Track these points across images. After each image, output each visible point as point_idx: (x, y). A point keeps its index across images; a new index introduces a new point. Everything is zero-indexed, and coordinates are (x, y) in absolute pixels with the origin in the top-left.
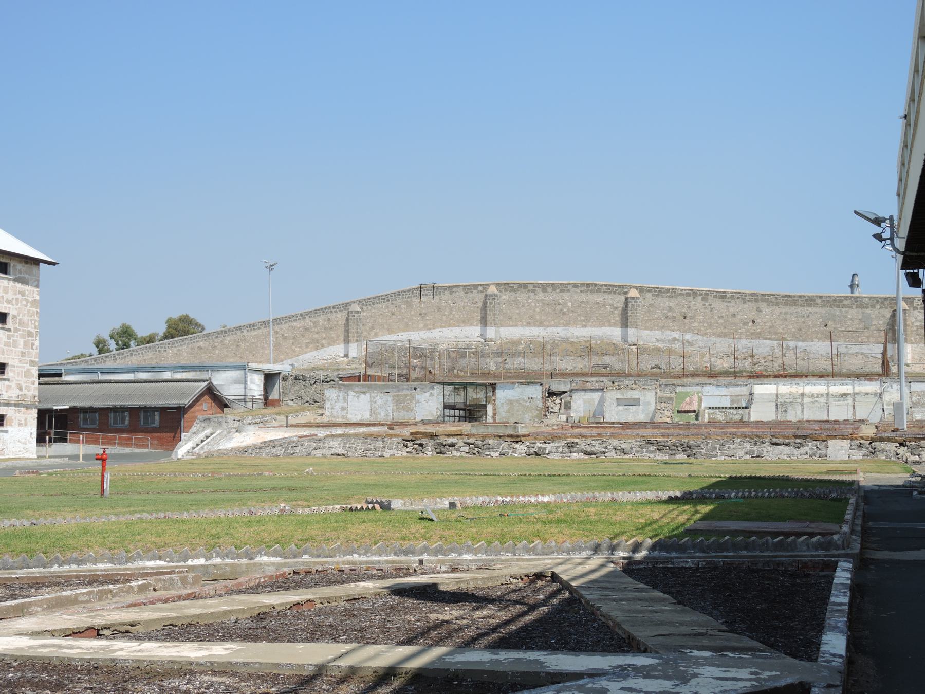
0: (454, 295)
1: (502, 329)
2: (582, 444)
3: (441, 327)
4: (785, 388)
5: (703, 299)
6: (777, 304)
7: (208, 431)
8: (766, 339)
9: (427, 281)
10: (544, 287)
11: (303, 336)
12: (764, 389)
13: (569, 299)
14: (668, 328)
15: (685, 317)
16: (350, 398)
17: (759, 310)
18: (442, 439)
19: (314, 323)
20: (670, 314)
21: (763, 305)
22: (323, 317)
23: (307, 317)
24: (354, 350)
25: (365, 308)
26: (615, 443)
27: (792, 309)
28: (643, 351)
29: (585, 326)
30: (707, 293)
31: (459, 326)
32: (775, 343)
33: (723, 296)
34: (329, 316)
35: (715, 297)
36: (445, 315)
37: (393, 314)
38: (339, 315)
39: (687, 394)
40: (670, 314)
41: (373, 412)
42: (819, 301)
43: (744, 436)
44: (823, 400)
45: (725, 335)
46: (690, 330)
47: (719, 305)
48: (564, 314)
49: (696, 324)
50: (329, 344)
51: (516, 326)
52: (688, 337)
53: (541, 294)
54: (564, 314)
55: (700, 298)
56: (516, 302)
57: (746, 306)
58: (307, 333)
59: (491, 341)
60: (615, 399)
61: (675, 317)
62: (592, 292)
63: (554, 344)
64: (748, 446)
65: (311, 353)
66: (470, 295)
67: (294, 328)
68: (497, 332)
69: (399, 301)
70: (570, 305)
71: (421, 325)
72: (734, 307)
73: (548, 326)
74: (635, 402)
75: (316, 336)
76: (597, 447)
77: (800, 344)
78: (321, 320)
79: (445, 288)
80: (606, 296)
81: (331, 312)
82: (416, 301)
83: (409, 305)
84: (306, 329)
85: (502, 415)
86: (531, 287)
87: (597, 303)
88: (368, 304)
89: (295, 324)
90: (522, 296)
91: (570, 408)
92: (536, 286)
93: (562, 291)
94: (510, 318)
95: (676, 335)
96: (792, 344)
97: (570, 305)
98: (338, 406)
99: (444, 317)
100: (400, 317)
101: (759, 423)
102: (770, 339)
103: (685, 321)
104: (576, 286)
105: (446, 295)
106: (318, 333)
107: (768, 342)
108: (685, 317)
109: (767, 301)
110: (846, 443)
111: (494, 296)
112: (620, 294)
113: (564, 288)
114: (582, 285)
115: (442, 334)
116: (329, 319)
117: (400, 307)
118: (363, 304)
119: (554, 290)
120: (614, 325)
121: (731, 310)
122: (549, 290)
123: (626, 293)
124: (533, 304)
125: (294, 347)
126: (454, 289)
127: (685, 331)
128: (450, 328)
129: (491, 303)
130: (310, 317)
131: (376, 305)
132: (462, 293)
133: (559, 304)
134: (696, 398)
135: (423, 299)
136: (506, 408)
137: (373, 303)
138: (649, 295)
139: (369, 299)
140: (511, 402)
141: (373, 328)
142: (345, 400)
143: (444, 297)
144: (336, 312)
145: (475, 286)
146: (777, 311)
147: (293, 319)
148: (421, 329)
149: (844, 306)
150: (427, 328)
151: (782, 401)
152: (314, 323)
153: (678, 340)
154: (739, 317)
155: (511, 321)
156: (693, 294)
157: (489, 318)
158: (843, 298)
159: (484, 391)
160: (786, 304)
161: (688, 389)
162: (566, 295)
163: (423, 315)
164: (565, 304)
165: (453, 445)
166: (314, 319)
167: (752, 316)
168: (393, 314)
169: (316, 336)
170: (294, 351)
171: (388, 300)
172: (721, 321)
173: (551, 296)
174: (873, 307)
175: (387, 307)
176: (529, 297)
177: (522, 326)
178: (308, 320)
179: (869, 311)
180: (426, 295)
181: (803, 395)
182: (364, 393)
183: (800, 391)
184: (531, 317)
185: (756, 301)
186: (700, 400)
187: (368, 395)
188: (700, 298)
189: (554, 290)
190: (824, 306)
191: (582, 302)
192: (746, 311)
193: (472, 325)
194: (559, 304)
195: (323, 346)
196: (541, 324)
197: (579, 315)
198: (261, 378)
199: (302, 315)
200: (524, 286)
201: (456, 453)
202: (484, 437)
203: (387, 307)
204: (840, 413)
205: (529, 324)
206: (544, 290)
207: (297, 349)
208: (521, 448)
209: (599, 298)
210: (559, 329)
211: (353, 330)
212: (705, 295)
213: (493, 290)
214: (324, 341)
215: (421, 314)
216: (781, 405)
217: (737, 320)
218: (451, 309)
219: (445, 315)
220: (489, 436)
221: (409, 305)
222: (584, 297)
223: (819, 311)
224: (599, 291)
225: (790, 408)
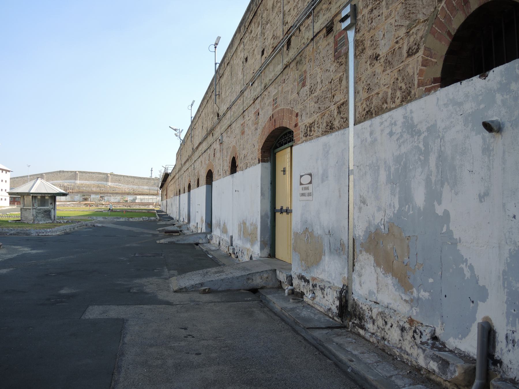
4: (142, 197)
9: (62, 170)
10: (89, 173)
17: (134, 180)
21: (135, 179)
26: (118, 205)
27: (141, 180)
30: (124, 176)
33: (127, 177)
43: (138, 205)
45: (127, 184)
46: (121, 183)
47: (126, 178)
52: (120, 184)
64: (138, 206)
72: (129, 179)
74: (116, 199)
76: (116, 206)
77: (142, 187)
82: (59, 174)
83: (57, 175)
85: (92, 200)
90: (84, 174)
92: (87, 172)
95: (117, 184)
96: (141, 187)
101: (137, 203)
105: (66, 173)
110: (152, 206)
140: (93, 198)
141: (48, 179)
145: (73, 171)
146: (138, 180)
162: (94, 175)
173: (91, 175)
178: (32, 177)
179: (155, 181)
192: (132, 180)
196: (88, 180)
204: (150, 201)
205: (85, 180)
208: (104, 206)
210: (92, 182)
212: (124, 176)
216: (141, 200)
222: (98, 175)
223: (146, 181)
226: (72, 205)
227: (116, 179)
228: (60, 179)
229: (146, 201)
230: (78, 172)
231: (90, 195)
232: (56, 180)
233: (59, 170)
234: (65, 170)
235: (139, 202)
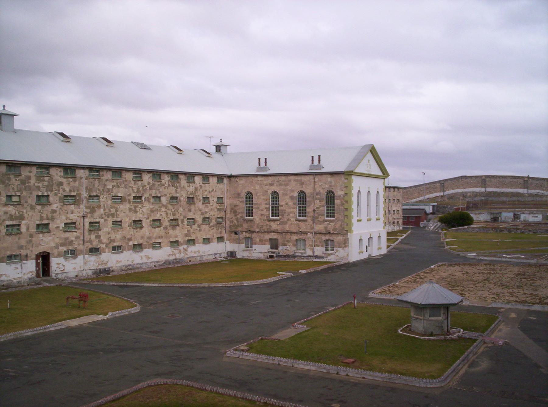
15: (541, 186)
19: (430, 186)
29: (511, 188)
34: (435, 184)
37: (454, 184)
49: (544, 188)
50: (434, 193)
55: (546, 181)
56: (491, 181)
62: (514, 178)
66: (477, 179)
70: (507, 182)
73: (501, 188)
78: (432, 186)
80: (518, 180)
82: (460, 180)
83: (458, 181)
86: (495, 177)
87: (515, 182)
90: (492, 180)
97: (507, 182)
105: (469, 179)
112: (522, 179)
123: (524, 179)
133: (504, 182)
138: (531, 180)
152: (430, 186)
162: (506, 179)
163: (463, 185)
164: (506, 182)
168: (454, 184)
170: (424, 194)
173: (501, 180)
175: (452, 182)
178: (428, 185)
180: (464, 179)
188: (546, 181)
189: (502, 178)
191: (511, 181)
194: (504, 182)
195: (433, 193)
196: (498, 188)
198: (432, 206)
201: (504, 232)
203: (452, 182)
206: (499, 178)
207: (425, 194)
209: (515, 180)
214: (433, 192)
221: (458, 181)
222: (511, 180)
224: (516, 178)
228: (462, 187)
231: (501, 213)
232: (458, 188)
233: (461, 176)
234: (467, 175)
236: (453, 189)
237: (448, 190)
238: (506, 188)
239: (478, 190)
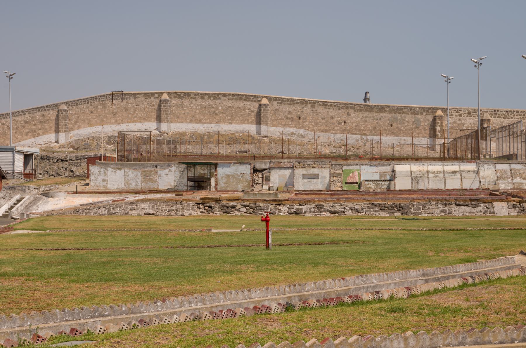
0: (137, 100)
1: (172, 125)
2: (327, 206)
3: (128, 122)
4: (416, 167)
5: (312, 106)
6: (361, 111)
7: (18, 197)
8: (353, 134)
9: (117, 89)
10: (202, 96)
11: (24, 127)
12: (401, 168)
13: (220, 105)
14: (288, 126)
15: (299, 118)
16: (109, 173)
17: (349, 114)
18: (225, 203)
20: (289, 116)
21: (351, 111)
22: (39, 114)
23: (27, 113)
24: (63, 138)
25: (71, 107)
26: (351, 205)
27: (370, 114)
28: (272, 141)
29: (231, 123)
30: (314, 102)
31: (140, 122)
32: (359, 136)
33: (325, 104)
34: (43, 113)
35: (320, 105)
36: (130, 114)
37: (92, 112)
38: (51, 112)
39: (350, 171)
40: (289, 116)
41: (127, 183)
42: (387, 109)
43: (437, 200)
44: (441, 175)
45: (326, 131)
46: (303, 127)
47: (322, 110)
48: (216, 114)
49: (307, 123)
50: (44, 134)
51: (182, 122)
52: (302, 131)
53: (200, 100)
54: (216, 114)
55: (310, 105)
56: (182, 105)
57: (340, 111)
58: (26, 125)
59: (164, 133)
60: (301, 174)
61: (292, 118)
62: (236, 100)
63: (210, 135)
64: (441, 207)
65: (30, 140)
66: (149, 100)
67: (17, 121)
68: (169, 126)
69: (96, 103)
70: (220, 108)
71: (113, 121)
72: (333, 112)
73: (205, 123)
74: (316, 177)
75: (34, 127)
76: (338, 208)
78: (38, 115)
79: (131, 95)
80: (246, 103)
81: (45, 110)
82: (109, 103)
83: (104, 106)
84: (26, 122)
85: (222, 184)
86: (193, 95)
87: (239, 108)
88: (73, 105)
89: (17, 118)
90: (186, 101)
91: (269, 180)
92: (197, 94)
93: (215, 99)
94: (178, 117)
95: (293, 130)
96: (369, 137)
97: (220, 108)
98: (100, 178)
99: (130, 115)
100: (97, 115)
101: (401, 192)
102: (356, 134)
103: (300, 121)
104: (225, 95)
105: (132, 99)
106: (35, 125)
107: (354, 136)
108: (299, 118)
109: (354, 108)
110: (505, 204)
111: (166, 101)
112: (255, 101)
113: (216, 96)
114: (229, 94)
115: (128, 127)
116: (43, 115)
117: (97, 107)
118: (69, 105)
119: (209, 97)
120: (251, 123)
121: (331, 114)
122: (206, 97)
123: (259, 101)
124: (194, 107)
125: (16, 135)
126: (137, 96)
127: (300, 128)
128: (135, 123)
129: (164, 106)
130: (29, 113)
131: (79, 106)
132: (143, 98)
133: (213, 108)
134: (356, 174)
135: (114, 102)
136: (224, 180)
137: (77, 104)
138: (275, 103)
139: (74, 101)
140: (228, 176)
141: (76, 122)
142: (105, 174)
143: (130, 101)
144: (49, 110)
145: (153, 94)
146: (361, 115)
147: (16, 115)
148: (113, 124)
149: (403, 113)
150: (117, 123)
151: (415, 176)
152: (32, 118)
153: (295, 134)
154: (336, 119)
155: (178, 119)
156: (305, 102)
157: (163, 116)
158: (403, 108)
159: (208, 168)
160: (366, 111)
161: (351, 168)
162: (218, 102)
163: (114, 114)
164: (217, 108)
165: (234, 207)
166: (32, 115)
167: (343, 118)
168: (92, 112)
169: (34, 127)
170: (17, 138)
171: (88, 103)
172: (324, 121)
174: (422, 114)
175: (87, 107)
176: (191, 102)
177: (186, 122)
178: (27, 115)
179: (419, 116)
180: (117, 99)
181: (428, 172)
182: (120, 169)
183: (426, 169)
184: (193, 116)
185: (347, 108)
186: (360, 175)
187: (123, 171)
188: (310, 105)
189: (209, 97)
190: (390, 112)
191: (229, 107)
192: (340, 115)
193: (150, 121)
194: (213, 108)
195: (39, 135)
196: (200, 121)
197: (227, 116)
198: (22, 157)
199: (22, 112)
200: (188, 94)
202: (255, 202)
203: (87, 107)
205: (191, 121)
206: (202, 98)
207: (19, 137)
208: (284, 209)
209: (241, 104)
210: (213, 125)
211: (62, 123)
212: (313, 104)
213: (165, 96)
214: (40, 131)
215: (113, 113)
216: (415, 179)
217: (334, 121)
218: (135, 110)
219: (130, 114)
220: (258, 200)
221: (104, 106)
222: (230, 103)
223: (387, 116)
224: (241, 99)
225: (420, 181)
226: (145, 206)
227: (290, 112)
228: (113, 121)
229: (433, 185)
230: (169, 93)
235: (408, 187)
236: (90, 124)
237: (79, 127)
238: (218, 122)
239: (151, 126)
